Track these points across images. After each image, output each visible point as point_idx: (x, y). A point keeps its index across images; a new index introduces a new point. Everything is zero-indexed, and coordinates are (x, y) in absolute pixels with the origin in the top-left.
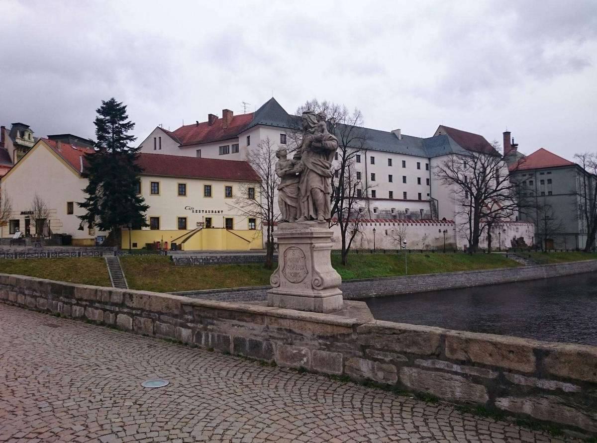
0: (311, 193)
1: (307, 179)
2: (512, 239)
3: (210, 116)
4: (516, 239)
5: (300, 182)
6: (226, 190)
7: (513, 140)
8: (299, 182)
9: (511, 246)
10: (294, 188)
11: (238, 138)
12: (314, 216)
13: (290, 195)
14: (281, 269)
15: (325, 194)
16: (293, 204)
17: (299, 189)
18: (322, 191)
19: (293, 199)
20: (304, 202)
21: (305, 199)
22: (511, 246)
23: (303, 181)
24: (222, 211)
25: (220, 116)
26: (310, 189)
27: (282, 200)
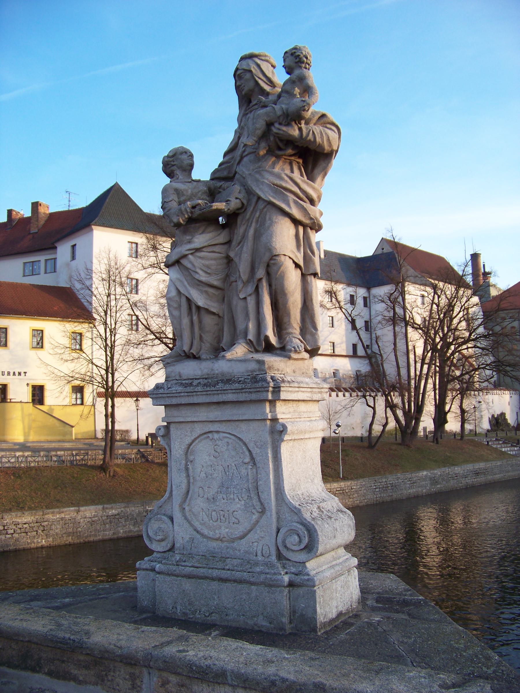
0: (268, 274)
1: (256, 231)
2: (490, 417)
3: (10, 212)
4: (496, 416)
5: (234, 243)
6: (34, 336)
7: (484, 265)
8: (229, 243)
9: (489, 428)
10: (215, 259)
11: (56, 248)
12: (273, 340)
13: (203, 277)
14: (177, 499)
15: (303, 275)
16: (214, 307)
17: (229, 260)
18: (297, 266)
19: (211, 290)
20: (245, 298)
21: (250, 289)
22: (489, 428)
23: (244, 236)
24: (25, 373)
25: (27, 213)
26: (266, 258)
27: (179, 292)
